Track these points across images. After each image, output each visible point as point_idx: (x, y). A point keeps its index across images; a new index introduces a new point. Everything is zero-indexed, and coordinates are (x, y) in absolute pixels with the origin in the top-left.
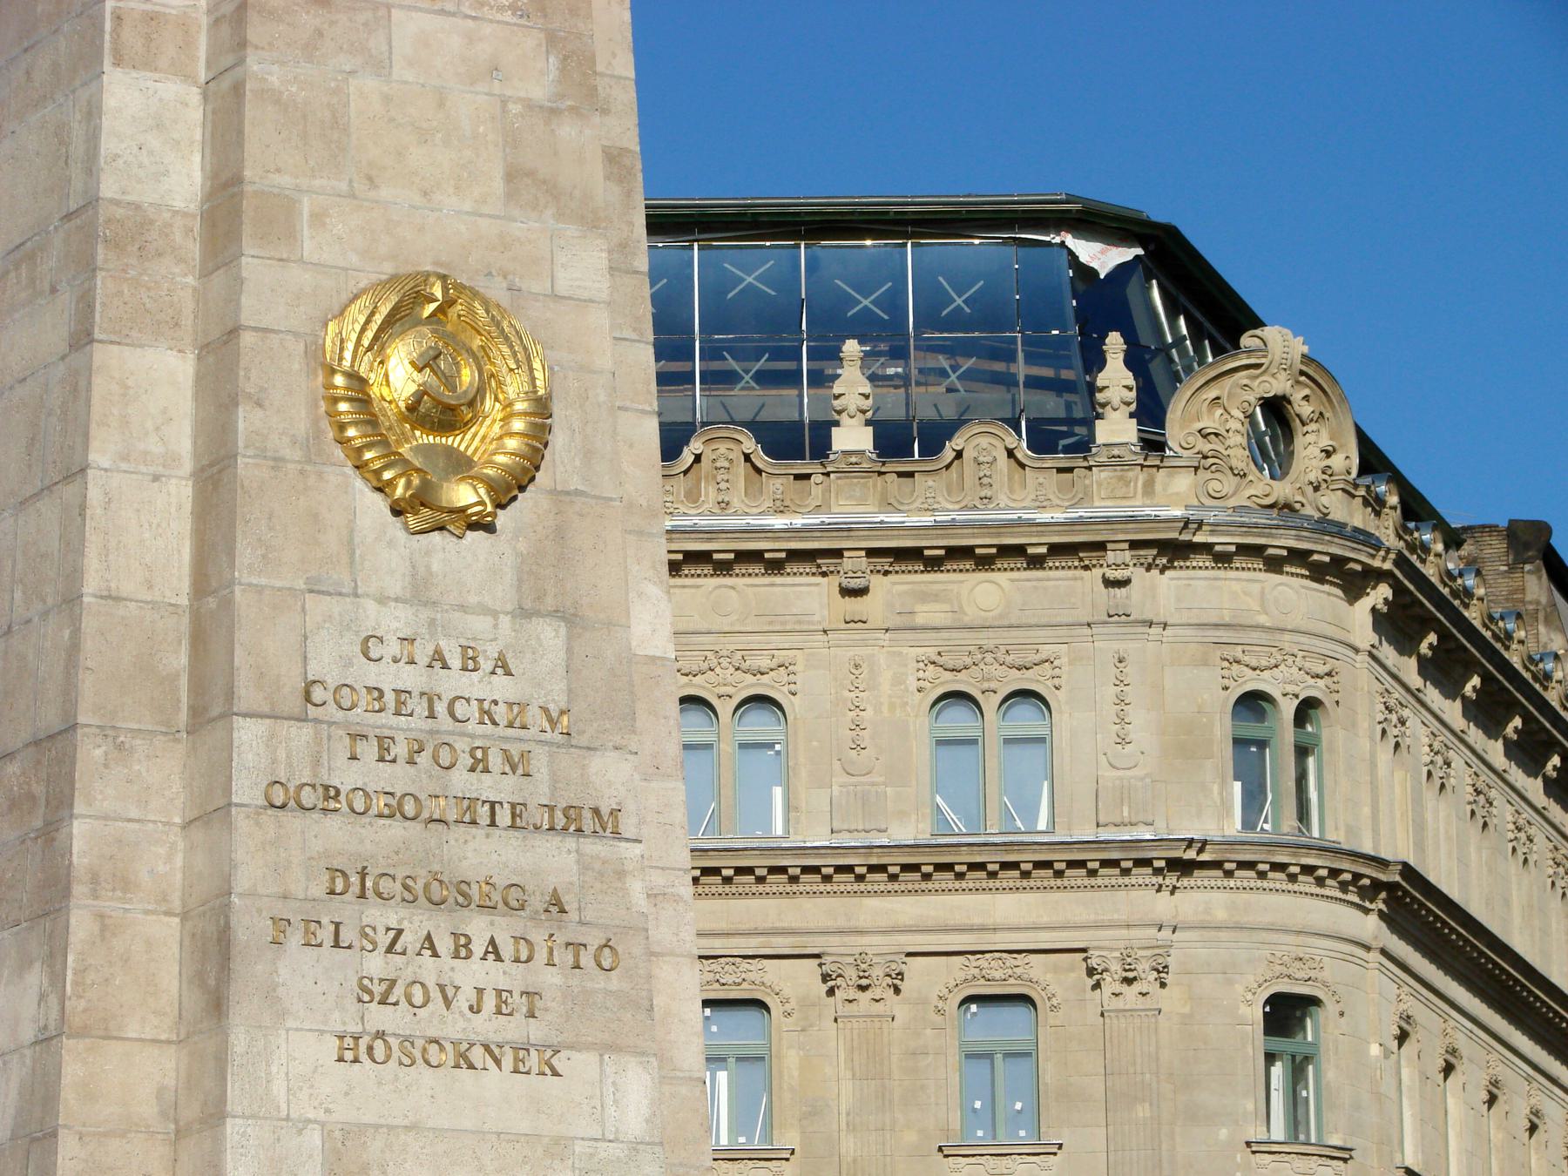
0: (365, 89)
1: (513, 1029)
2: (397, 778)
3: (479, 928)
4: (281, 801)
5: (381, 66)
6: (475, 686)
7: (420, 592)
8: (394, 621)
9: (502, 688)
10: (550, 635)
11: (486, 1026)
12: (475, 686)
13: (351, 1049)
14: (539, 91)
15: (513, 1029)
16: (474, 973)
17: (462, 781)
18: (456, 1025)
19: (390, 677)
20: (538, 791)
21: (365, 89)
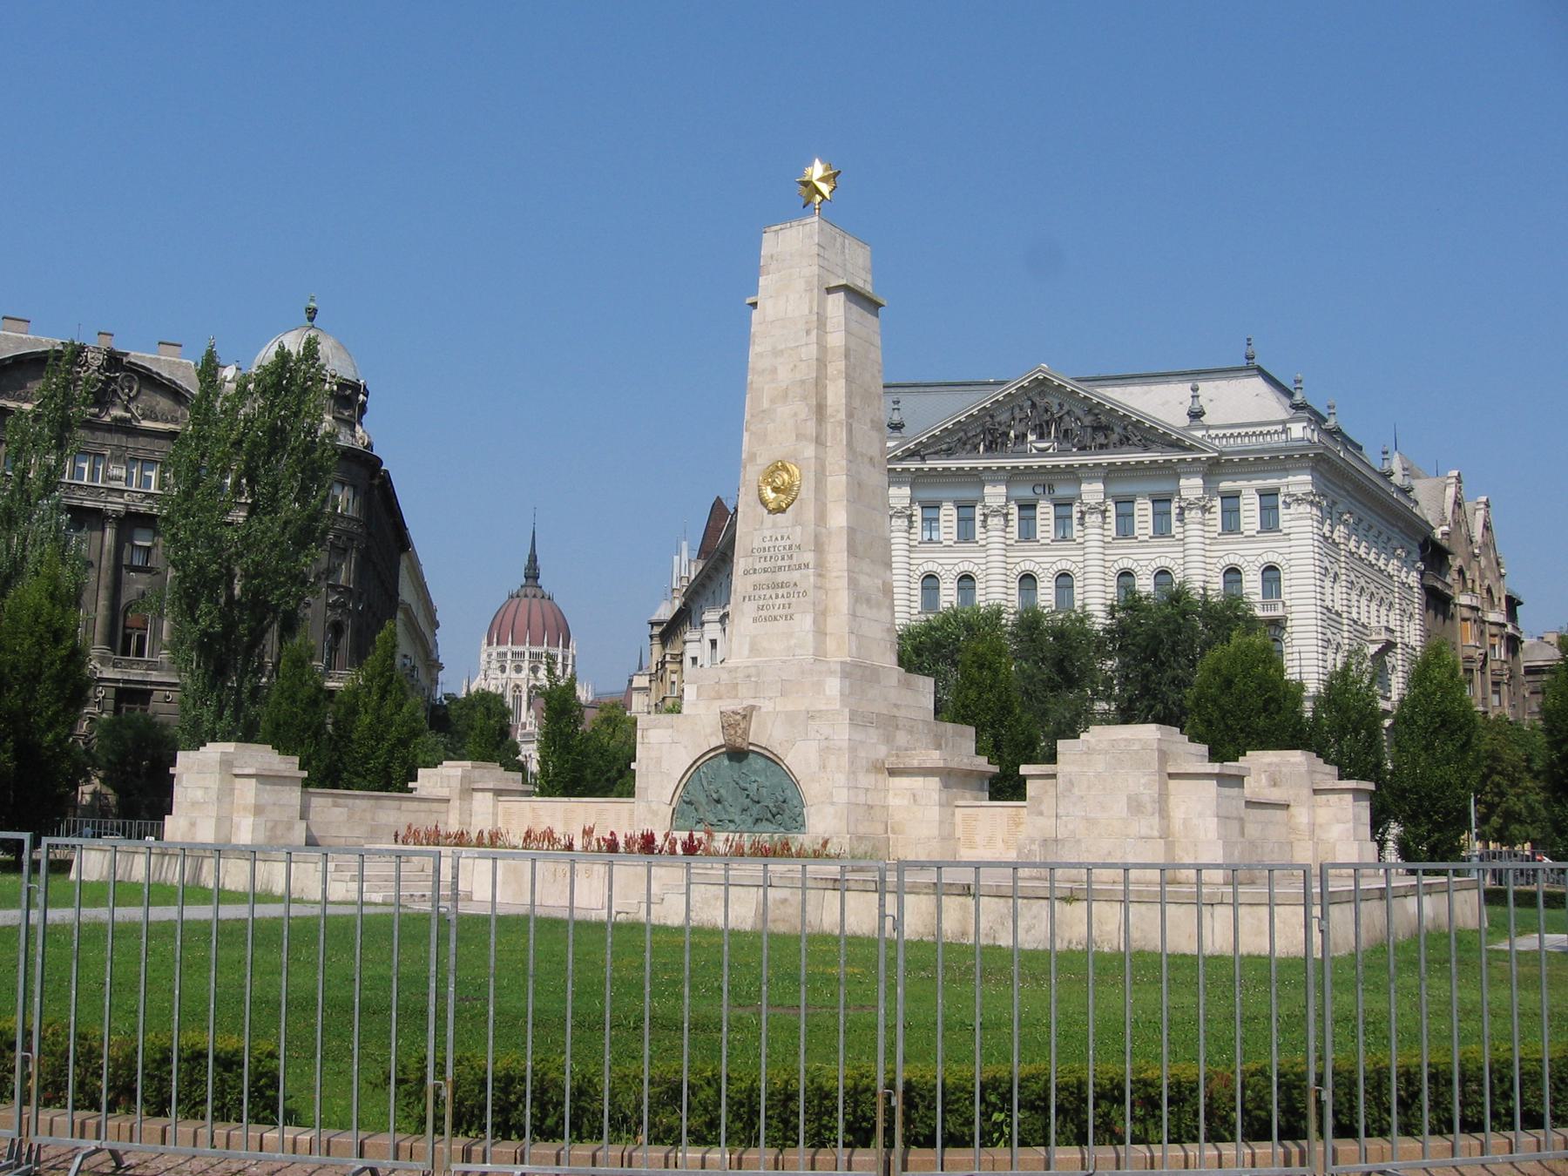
0: (771, 427)
1: (786, 611)
2: (767, 564)
3: (780, 592)
4: (746, 573)
5: (773, 421)
6: (783, 543)
7: (774, 526)
8: (767, 533)
9: (789, 542)
10: (798, 529)
11: (781, 612)
12: (783, 543)
13: (755, 620)
14: (803, 416)
15: (786, 611)
16: (780, 601)
17: (780, 563)
18: (776, 612)
19: (767, 545)
20: (794, 561)
21: (771, 427)
